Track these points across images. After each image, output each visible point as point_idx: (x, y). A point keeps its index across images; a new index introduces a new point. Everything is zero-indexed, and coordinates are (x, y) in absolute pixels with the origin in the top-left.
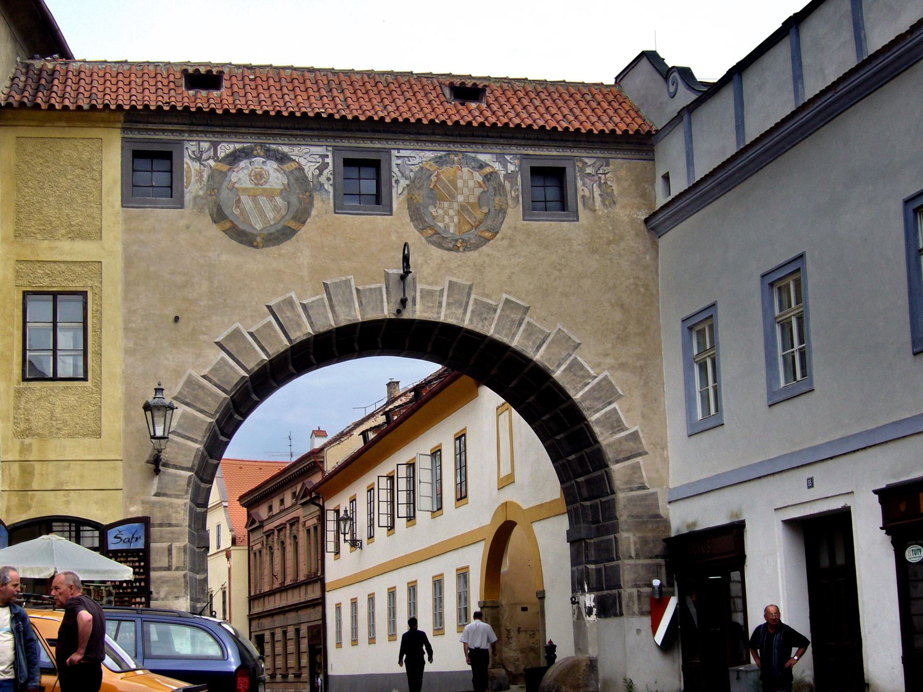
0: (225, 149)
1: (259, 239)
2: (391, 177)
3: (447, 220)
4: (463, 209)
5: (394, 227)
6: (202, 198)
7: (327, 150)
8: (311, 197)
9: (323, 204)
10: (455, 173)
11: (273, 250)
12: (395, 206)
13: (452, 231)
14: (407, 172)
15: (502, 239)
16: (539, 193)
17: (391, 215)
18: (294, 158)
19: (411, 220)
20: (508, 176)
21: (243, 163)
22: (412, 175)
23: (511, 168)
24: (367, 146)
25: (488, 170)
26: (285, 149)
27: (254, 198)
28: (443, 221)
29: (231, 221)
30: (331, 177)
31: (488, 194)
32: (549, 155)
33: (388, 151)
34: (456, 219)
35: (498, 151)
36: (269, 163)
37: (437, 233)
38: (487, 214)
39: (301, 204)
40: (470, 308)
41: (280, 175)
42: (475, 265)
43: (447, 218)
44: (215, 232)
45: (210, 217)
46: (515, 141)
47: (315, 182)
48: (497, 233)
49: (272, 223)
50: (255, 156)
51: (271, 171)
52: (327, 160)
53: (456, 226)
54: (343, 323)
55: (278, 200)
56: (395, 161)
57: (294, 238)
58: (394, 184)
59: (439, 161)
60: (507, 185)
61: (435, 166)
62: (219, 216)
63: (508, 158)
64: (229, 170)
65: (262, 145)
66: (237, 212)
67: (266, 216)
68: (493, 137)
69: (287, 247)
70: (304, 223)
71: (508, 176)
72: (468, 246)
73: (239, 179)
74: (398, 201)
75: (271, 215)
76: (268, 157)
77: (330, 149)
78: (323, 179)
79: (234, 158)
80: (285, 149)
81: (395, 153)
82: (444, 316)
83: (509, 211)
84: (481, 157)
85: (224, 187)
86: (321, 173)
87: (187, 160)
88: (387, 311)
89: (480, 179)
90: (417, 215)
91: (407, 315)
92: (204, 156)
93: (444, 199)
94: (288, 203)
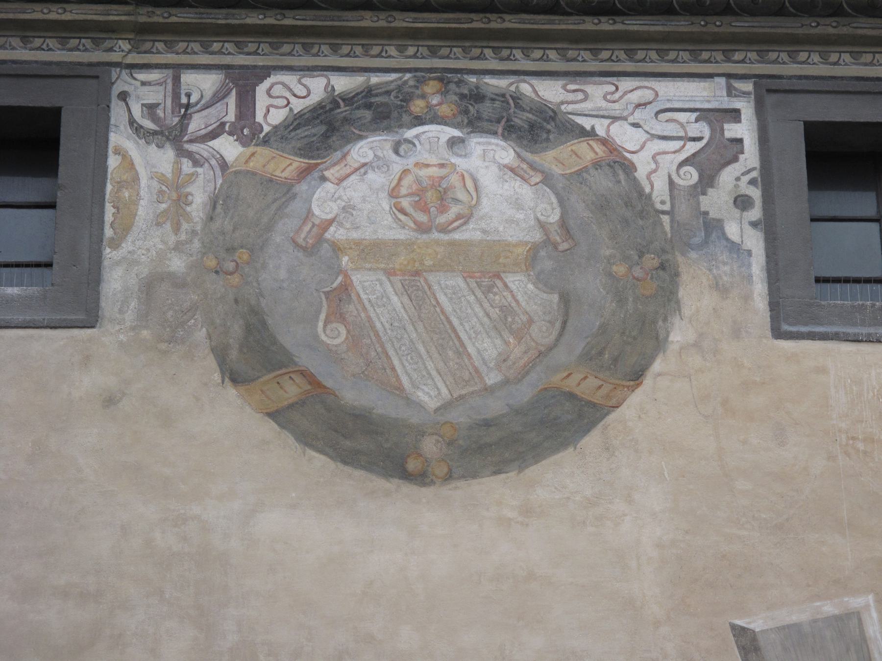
1: (430, 446)
6: (179, 283)
7: (731, 92)
8: (668, 274)
9: (721, 303)
11: (497, 493)
18: (586, 123)
21: (364, 149)
26: (551, 91)
27: (413, 279)
29: (304, 373)
30: (755, 193)
36: (478, 144)
39: (621, 301)
41: (526, 192)
44: (229, 418)
45: (211, 362)
47: (684, 211)
49: (492, 378)
50: (419, 121)
51: (488, 178)
52: (732, 130)
55: (519, 284)
57: (592, 440)
62: (253, 356)
64: (304, 173)
65: (444, 77)
66: (335, 336)
67: (462, 351)
69: (561, 477)
70: (637, 376)
73: (348, 209)
75: (485, 347)
77: (748, 86)
78: (717, 201)
79: (324, 131)
80: (551, 91)
85: (277, 238)
86: (707, 181)
87: (119, 138)
92: (197, 124)
94: (565, 299)
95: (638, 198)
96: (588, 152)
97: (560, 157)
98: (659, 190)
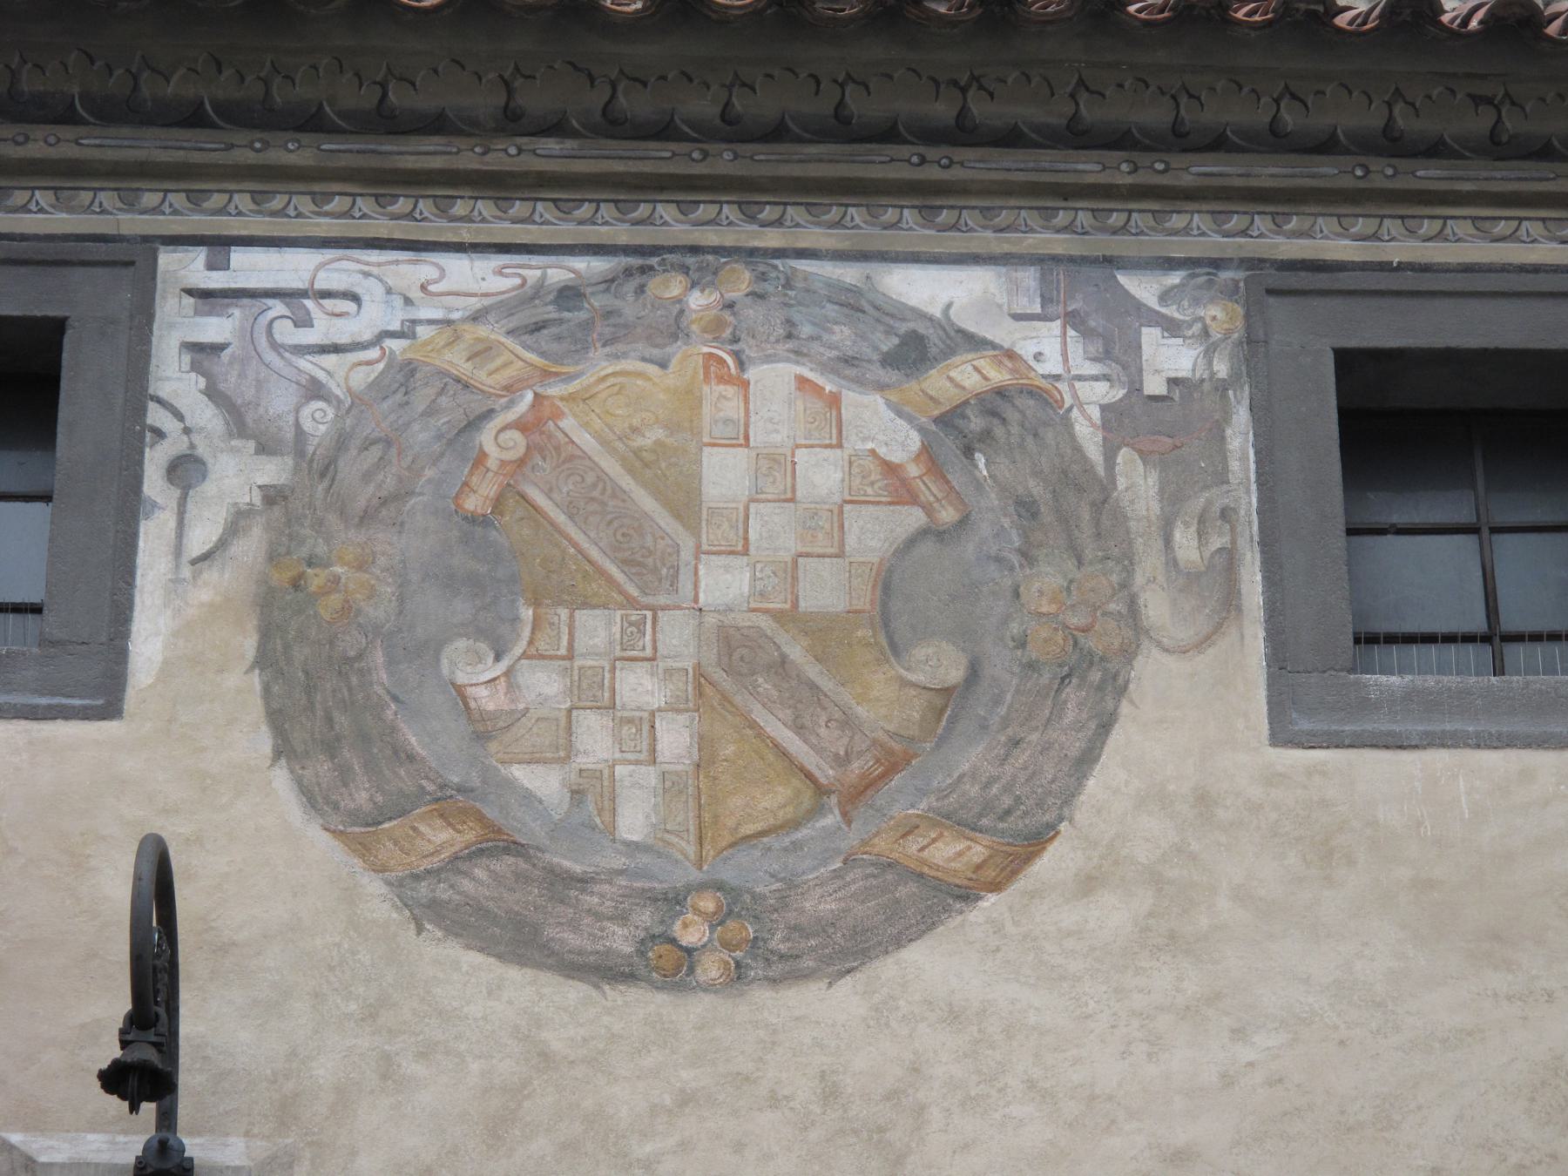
2: (134, 436)
3: (595, 740)
4: (738, 654)
10: (690, 399)
12: (149, 644)
13: (634, 822)
14: (280, 402)
15: (1088, 884)
16: (1432, 574)
17: (111, 709)
19: (283, 750)
20: (1137, 418)
22: (318, 420)
23: (1169, 359)
25: (967, 376)
28: (564, 752)
31: (969, 549)
33: (132, 260)
34: (675, 739)
35: (1060, 244)
37: (498, 843)
38: (948, 704)
42: (830, 1093)
43: (602, 732)
46: (1197, 170)
48: (1038, 840)
53: (670, 786)
56: (176, 326)
58: (154, 483)
60: (1138, 484)
61: (519, 356)
63: (1143, 288)
68: (1010, 138)
71: (1137, 418)
72: (772, 945)
74: (181, 605)
81: (185, 267)
83: (1152, 671)
84: (924, 289)
89: (900, 441)
90: (328, 702)
93: (566, 587)
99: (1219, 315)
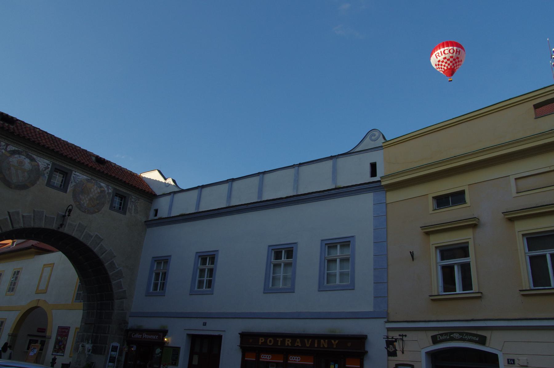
0: (11, 148)
5: (65, 199)
12: (68, 190)
13: (85, 205)
21: (16, 156)
23: (110, 191)
24: (66, 166)
25: (103, 189)
26: (35, 157)
32: (123, 190)
33: (72, 171)
36: (27, 159)
40: (84, 234)
54: (36, 226)
55: (26, 174)
56: (73, 175)
59: (88, 180)
60: (107, 196)
70: (33, 185)
71: (108, 193)
76: (27, 157)
78: (45, 172)
79: (13, 153)
80: (35, 157)
81: (74, 172)
82: (74, 234)
84: (102, 184)
86: (45, 170)
88: (54, 226)
91: (61, 230)
95: (39, 169)
96: (36, 164)
97: (33, 163)
98: (41, 169)
99: (112, 190)
